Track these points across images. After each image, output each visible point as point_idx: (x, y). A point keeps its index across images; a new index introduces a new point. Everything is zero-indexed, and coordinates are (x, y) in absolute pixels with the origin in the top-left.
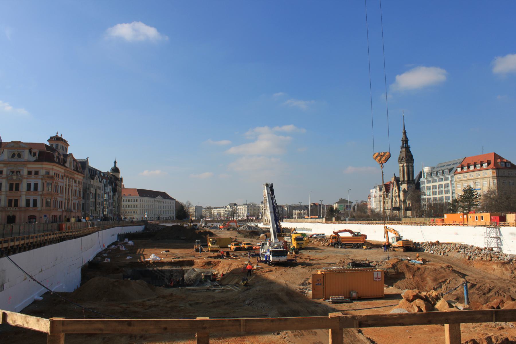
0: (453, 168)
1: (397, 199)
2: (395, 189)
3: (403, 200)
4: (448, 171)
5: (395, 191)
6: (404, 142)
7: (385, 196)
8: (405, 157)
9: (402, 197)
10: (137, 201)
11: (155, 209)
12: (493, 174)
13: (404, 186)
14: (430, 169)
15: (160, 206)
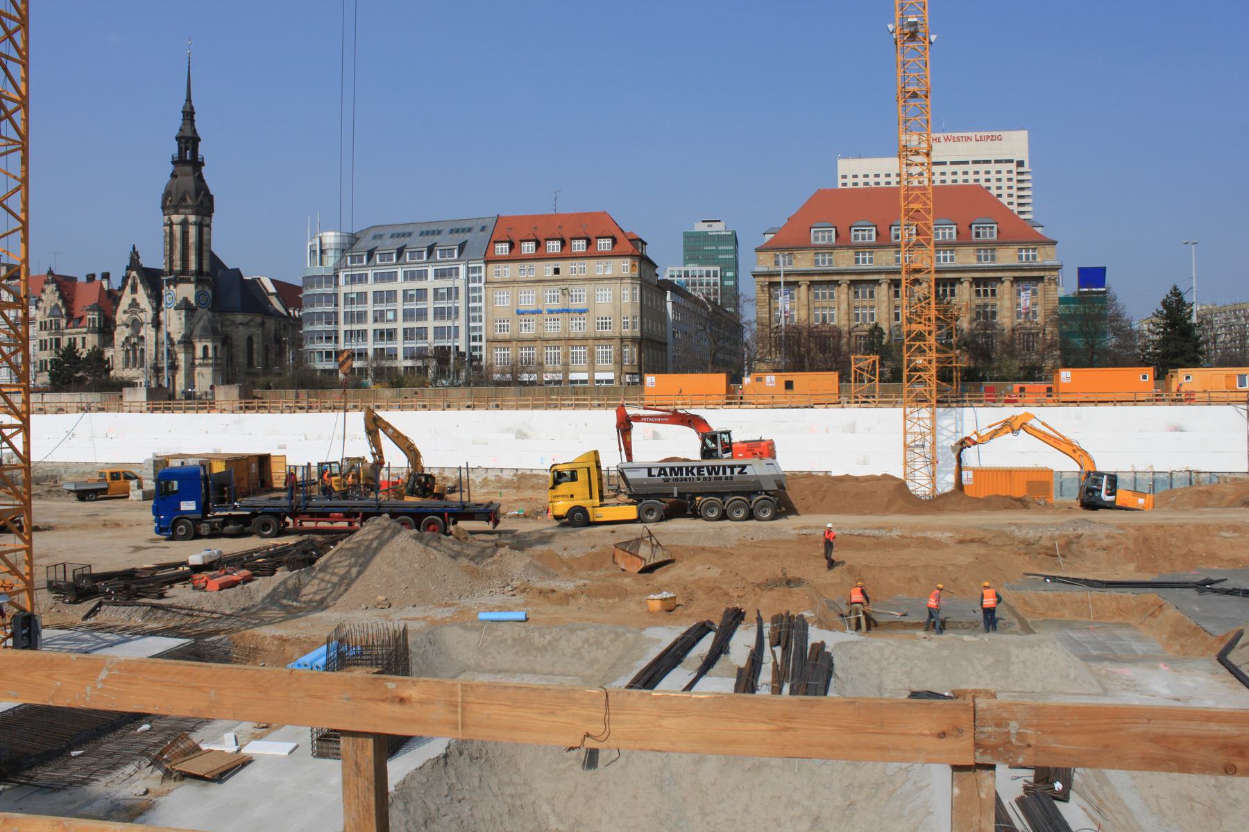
0: (466, 241)
1: (148, 332)
2: (134, 300)
3: (185, 336)
4: (394, 255)
5: (134, 304)
6: (187, 142)
7: (63, 322)
8: (193, 194)
9: (175, 323)
12: (632, 270)
13: (188, 291)
14: (347, 241)
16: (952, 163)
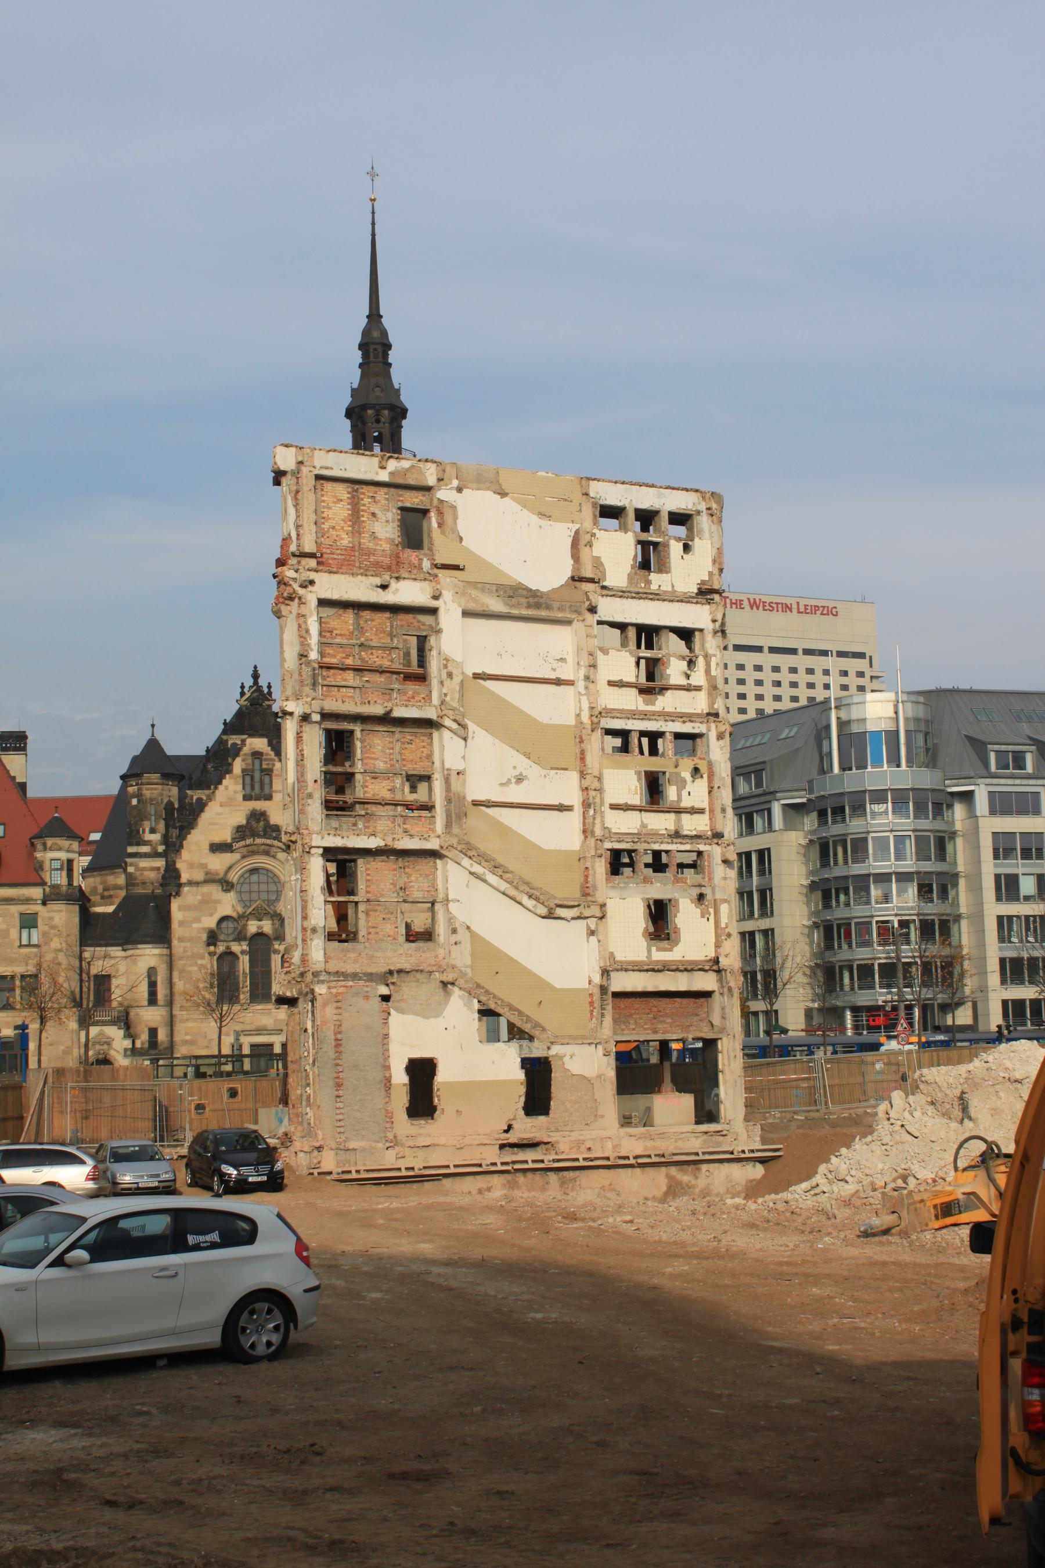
16: (773, 650)
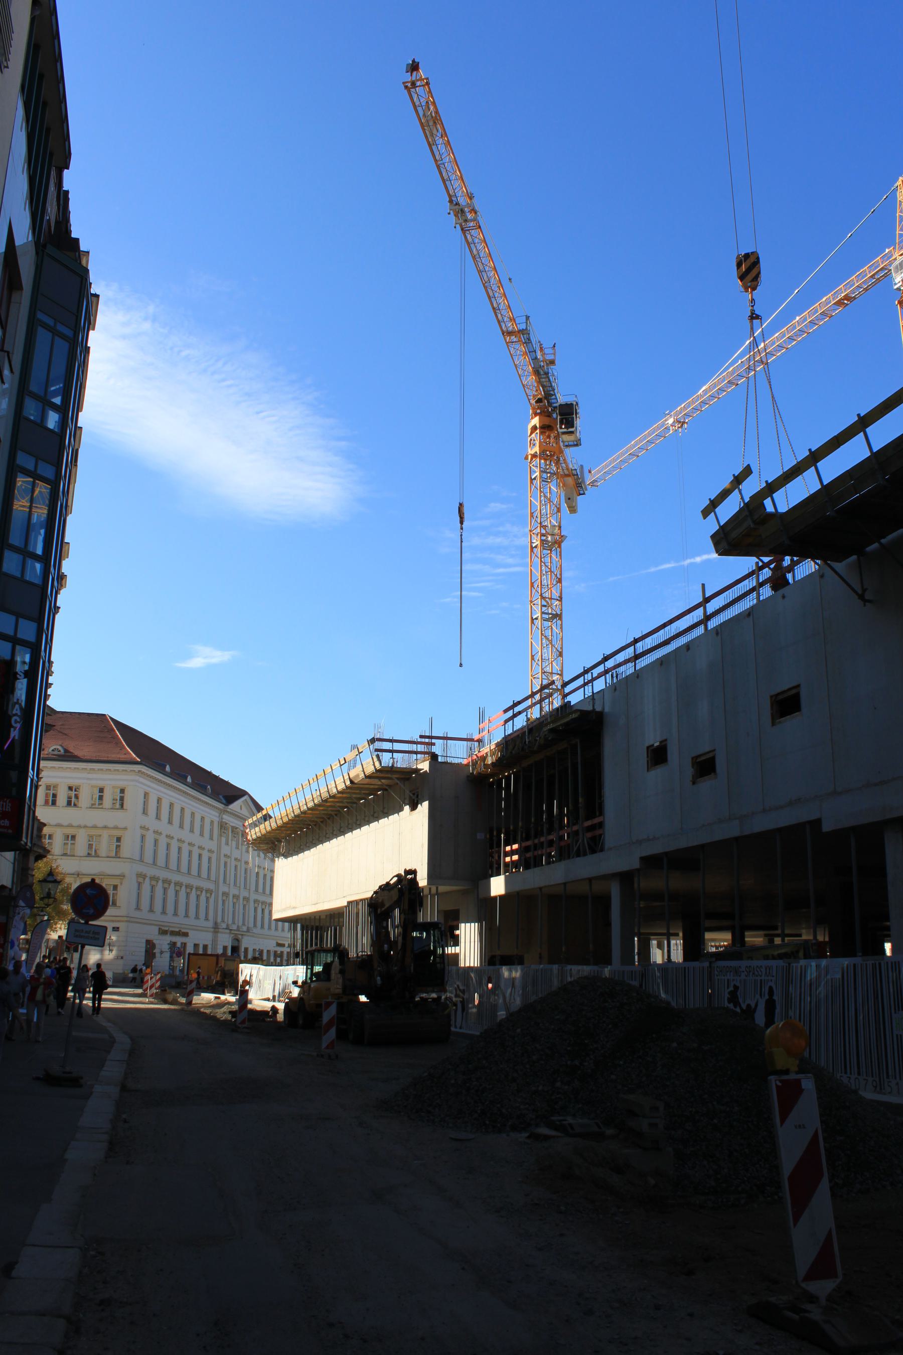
10: (121, 803)
11: (223, 888)
15: (234, 863)
